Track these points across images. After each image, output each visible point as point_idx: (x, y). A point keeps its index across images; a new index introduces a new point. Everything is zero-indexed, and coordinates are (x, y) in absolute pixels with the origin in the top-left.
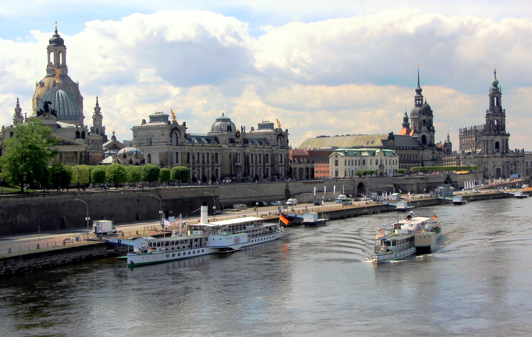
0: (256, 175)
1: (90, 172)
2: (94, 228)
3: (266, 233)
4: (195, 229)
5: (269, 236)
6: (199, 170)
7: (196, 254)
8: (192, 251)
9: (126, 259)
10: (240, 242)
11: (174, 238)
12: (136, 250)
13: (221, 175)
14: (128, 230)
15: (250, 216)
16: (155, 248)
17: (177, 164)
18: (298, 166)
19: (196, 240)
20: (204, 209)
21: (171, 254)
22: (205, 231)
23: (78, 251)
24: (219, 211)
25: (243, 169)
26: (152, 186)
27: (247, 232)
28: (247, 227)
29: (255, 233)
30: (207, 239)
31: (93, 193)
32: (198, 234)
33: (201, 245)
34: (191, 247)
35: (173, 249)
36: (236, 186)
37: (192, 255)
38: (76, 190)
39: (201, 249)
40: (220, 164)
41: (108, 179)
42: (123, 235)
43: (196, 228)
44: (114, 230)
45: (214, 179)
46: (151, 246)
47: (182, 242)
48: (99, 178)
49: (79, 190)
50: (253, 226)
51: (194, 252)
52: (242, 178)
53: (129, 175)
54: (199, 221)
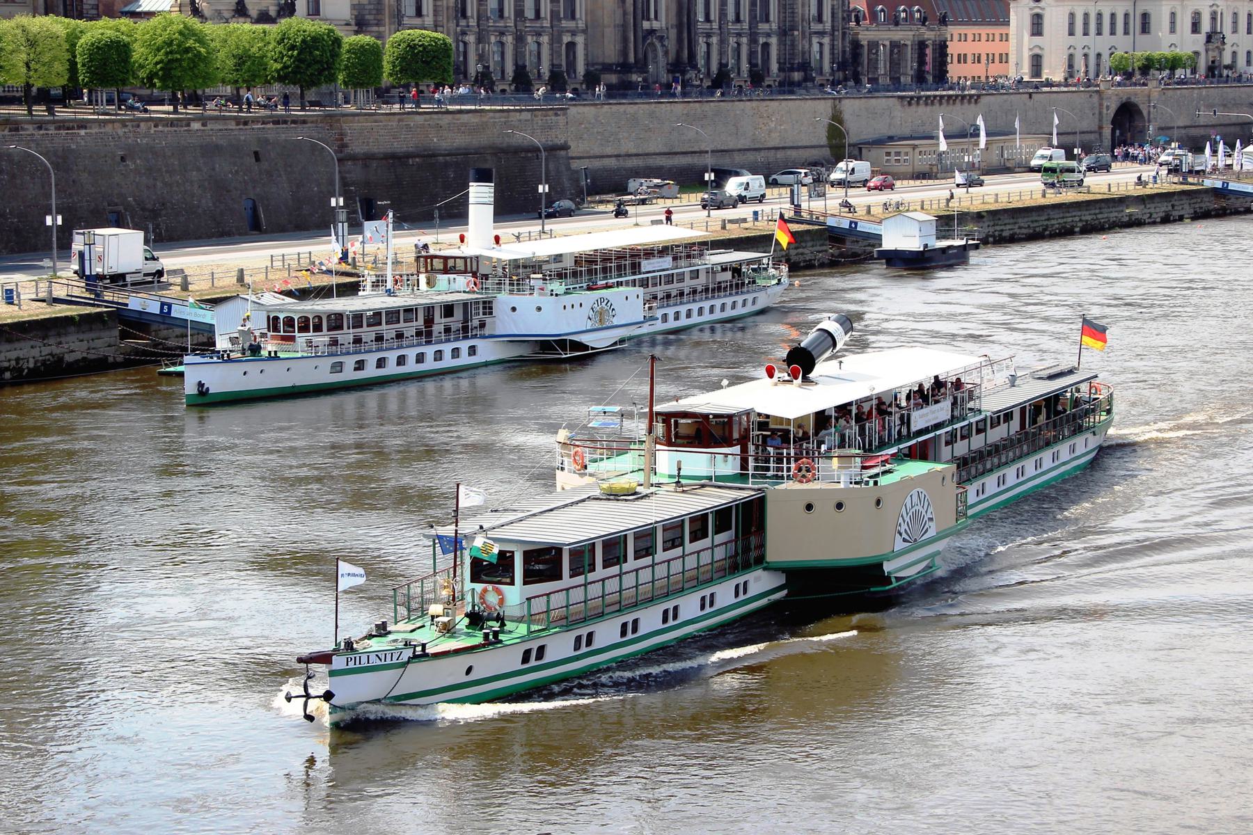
0: (722, 66)
1: (74, 45)
2: (75, 259)
3: (719, 289)
4: (446, 271)
5: (729, 301)
6: (502, 44)
7: (448, 362)
8: (429, 351)
9: (181, 374)
10: (616, 322)
11: (368, 301)
12: (222, 344)
13: (587, 64)
14: (202, 265)
15: (689, 220)
16: (292, 339)
17: (418, 21)
18: (886, 35)
19: (448, 310)
20: (480, 195)
21: (350, 362)
22: (486, 277)
23: (9, 341)
24: (566, 204)
25: (671, 44)
26: (312, 104)
27: (644, 283)
28: (646, 265)
29: (674, 288)
30: (488, 307)
31: (83, 124)
32: (455, 288)
33: (465, 329)
34: (426, 335)
35: (358, 341)
36: (639, 109)
37: (430, 364)
38: (18, 111)
39: (464, 345)
40: (581, 25)
41: (142, 74)
42: (185, 287)
43: (448, 266)
44: (153, 267)
45: (557, 82)
46: (276, 329)
47: (393, 315)
48: (110, 67)
49: (30, 111)
50: (667, 262)
51: (439, 355)
52: (665, 77)
53: (223, 59)
54: (462, 239)
